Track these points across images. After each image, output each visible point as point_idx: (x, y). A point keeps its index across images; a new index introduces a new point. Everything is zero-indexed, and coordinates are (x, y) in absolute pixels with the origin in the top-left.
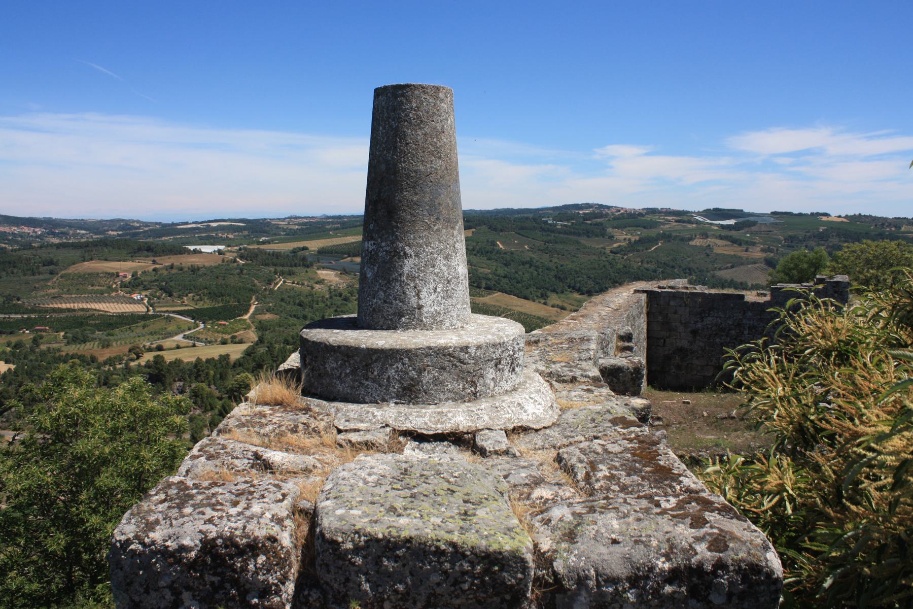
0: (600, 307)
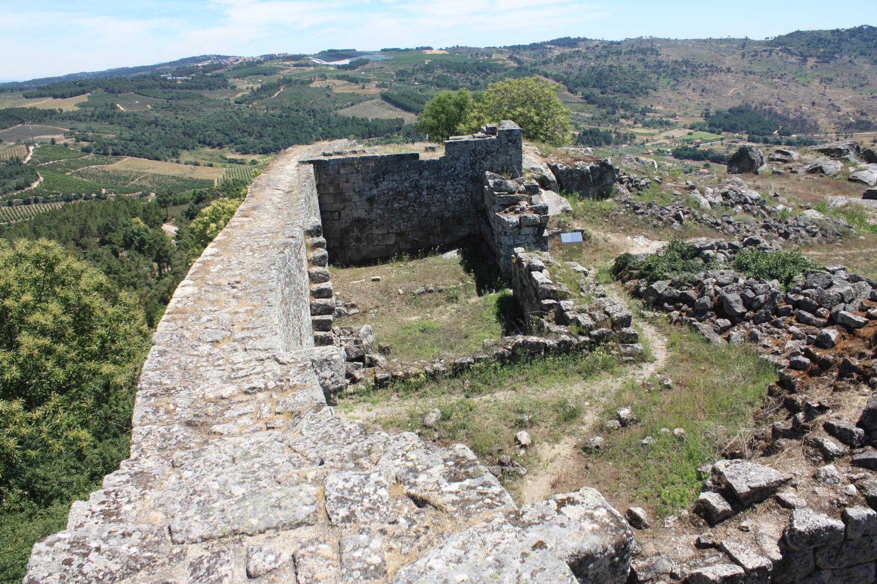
0: (268, 191)
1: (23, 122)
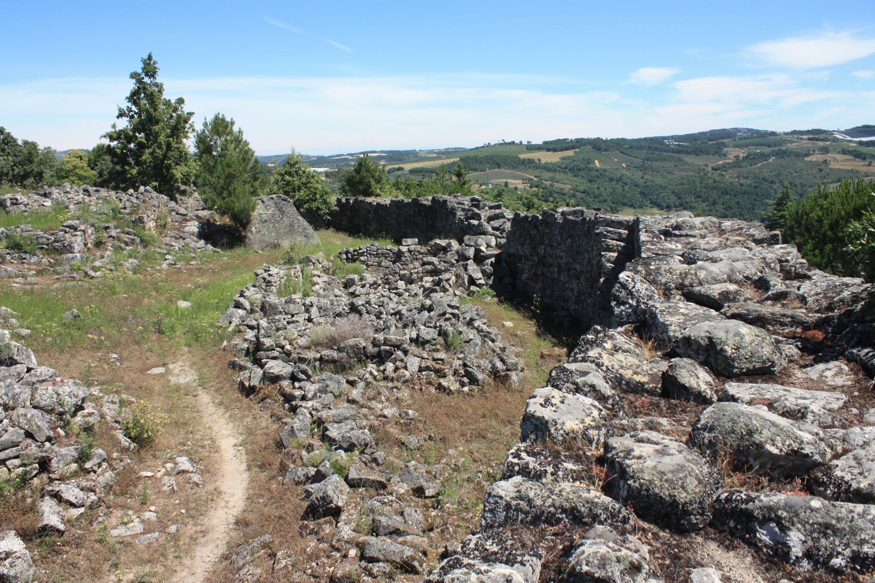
1: (499, 167)
